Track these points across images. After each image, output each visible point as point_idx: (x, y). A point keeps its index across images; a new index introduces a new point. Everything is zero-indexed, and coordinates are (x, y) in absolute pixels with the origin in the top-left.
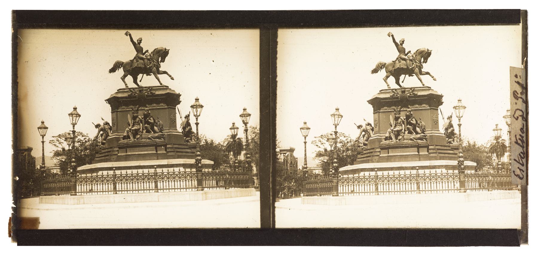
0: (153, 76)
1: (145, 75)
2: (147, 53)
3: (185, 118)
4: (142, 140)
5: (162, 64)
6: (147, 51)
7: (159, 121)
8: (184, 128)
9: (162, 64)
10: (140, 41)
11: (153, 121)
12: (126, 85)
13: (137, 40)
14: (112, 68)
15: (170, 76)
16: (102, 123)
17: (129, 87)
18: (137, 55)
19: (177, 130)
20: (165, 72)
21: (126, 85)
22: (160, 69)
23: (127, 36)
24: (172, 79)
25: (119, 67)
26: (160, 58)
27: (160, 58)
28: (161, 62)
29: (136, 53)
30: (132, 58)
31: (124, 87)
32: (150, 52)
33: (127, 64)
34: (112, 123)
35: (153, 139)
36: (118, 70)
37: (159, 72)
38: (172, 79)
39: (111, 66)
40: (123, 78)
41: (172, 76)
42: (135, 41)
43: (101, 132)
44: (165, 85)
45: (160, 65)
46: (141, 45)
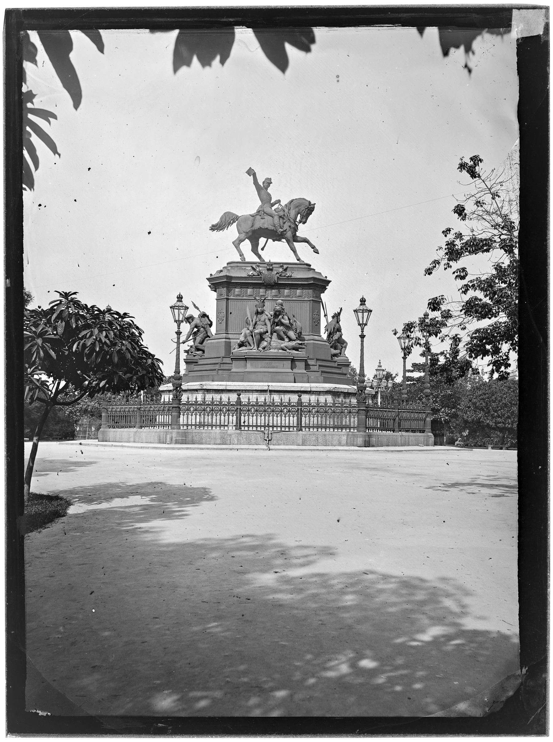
0: (283, 245)
1: (270, 241)
2: (278, 204)
3: (333, 317)
4: (271, 350)
5: (301, 226)
6: (279, 201)
7: (295, 321)
8: (330, 335)
9: (301, 226)
10: (268, 182)
11: (288, 322)
12: (241, 255)
13: (263, 183)
14: (217, 224)
15: (313, 247)
16: (196, 314)
17: (247, 260)
18: (261, 207)
19: (321, 336)
20: (306, 241)
21: (241, 255)
22: (298, 234)
23: (250, 176)
24: (317, 252)
25: (230, 224)
26: (299, 215)
27: (299, 215)
28: (300, 222)
29: (259, 203)
30: (254, 211)
31: (238, 259)
32: (283, 203)
33: (245, 218)
34: (217, 317)
35: (288, 350)
36: (228, 227)
37: (295, 239)
38: (317, 252)
39: (216, 221)
40: (237, 244)
41: (317, 247)
42: (261, 183)
43: (196, 330)
44: (306, 262)
45: (297, 226)
46: (269, 190)
